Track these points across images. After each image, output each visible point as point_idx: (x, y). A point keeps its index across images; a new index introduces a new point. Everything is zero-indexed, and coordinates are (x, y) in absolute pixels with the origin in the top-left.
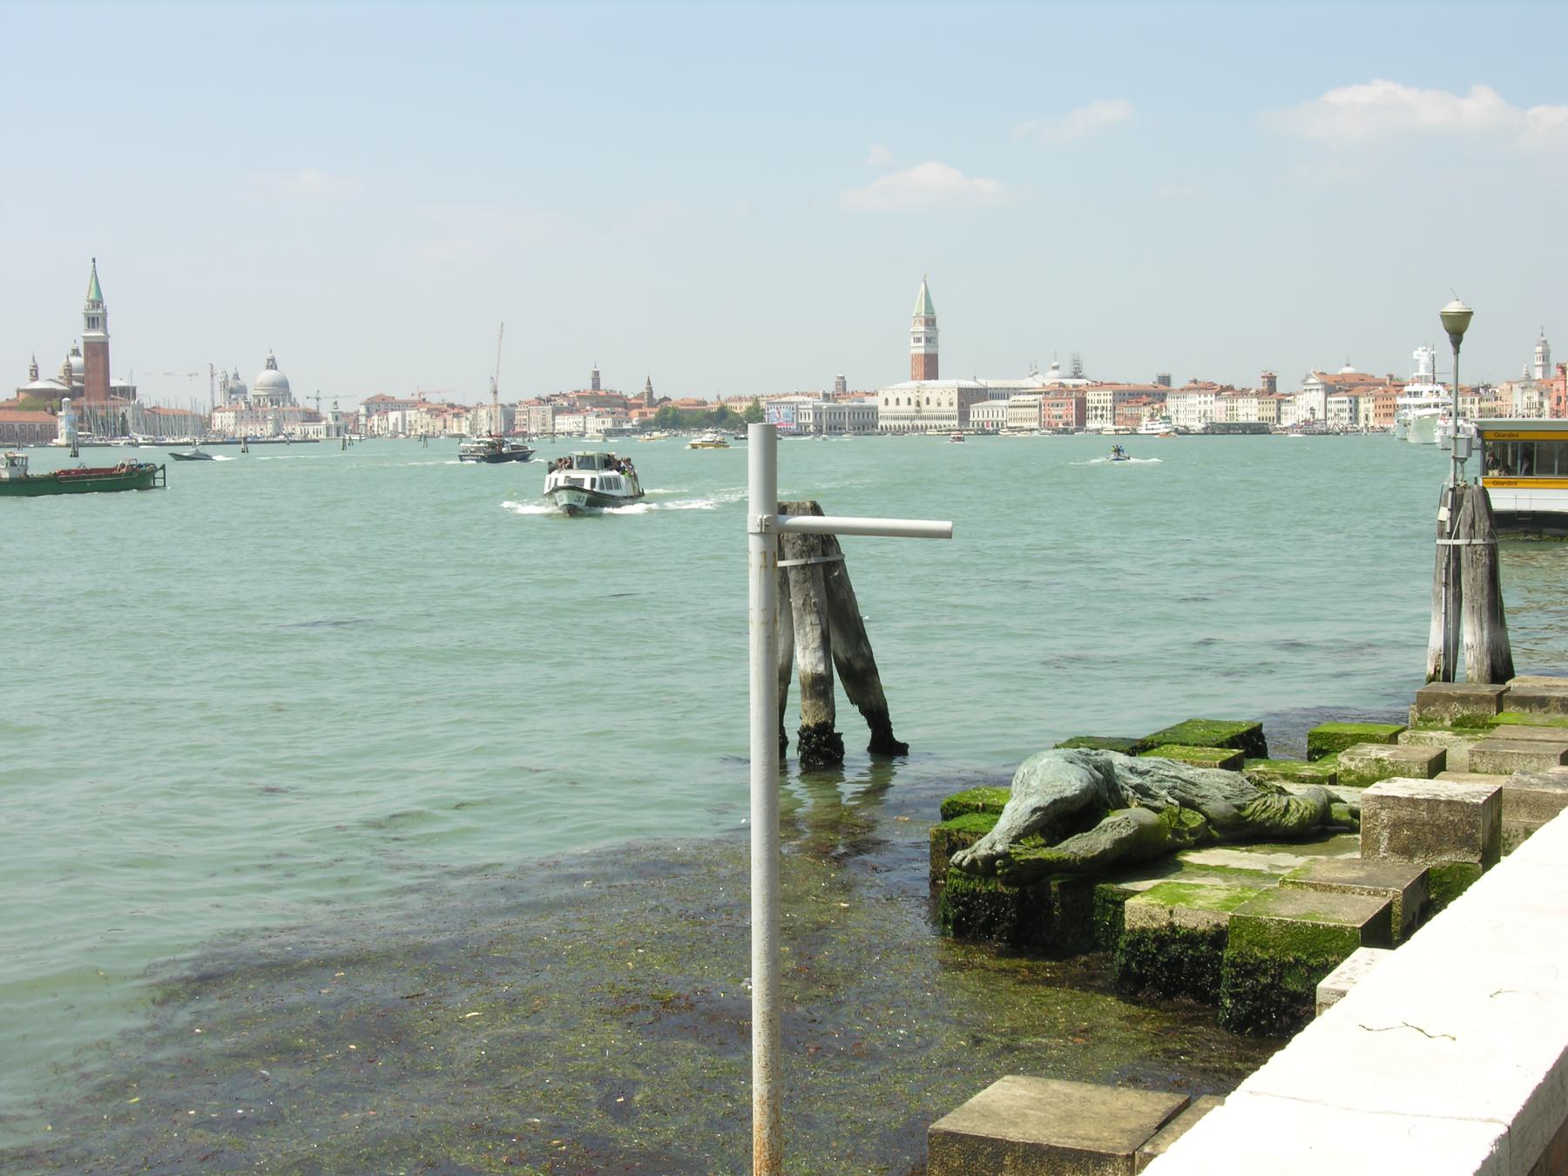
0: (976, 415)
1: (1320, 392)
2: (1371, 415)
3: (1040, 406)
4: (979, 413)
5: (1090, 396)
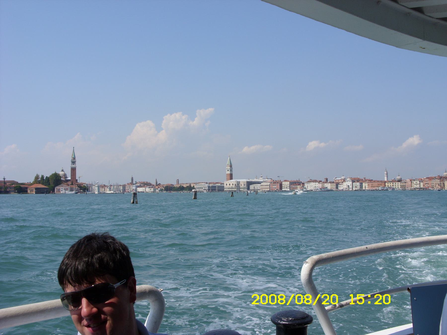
0: (252, 188)
1: (351, 182)
2: (367, 187)
3: (270, 185)
4: (252, 187)
5: (283, 183)
